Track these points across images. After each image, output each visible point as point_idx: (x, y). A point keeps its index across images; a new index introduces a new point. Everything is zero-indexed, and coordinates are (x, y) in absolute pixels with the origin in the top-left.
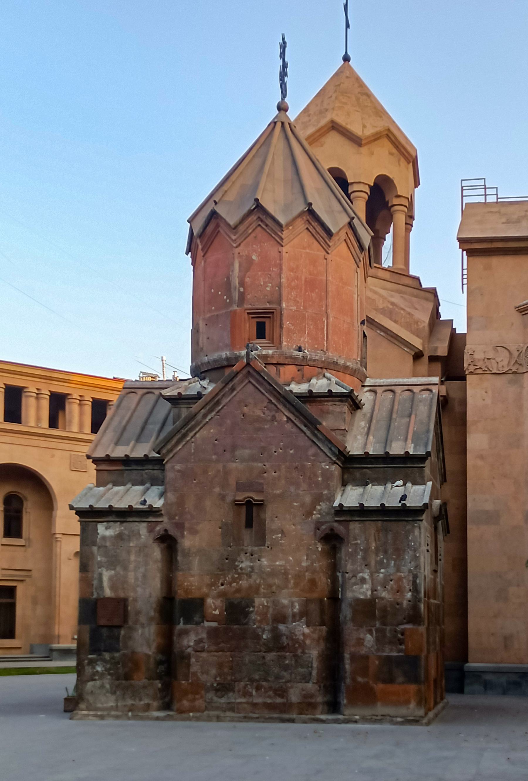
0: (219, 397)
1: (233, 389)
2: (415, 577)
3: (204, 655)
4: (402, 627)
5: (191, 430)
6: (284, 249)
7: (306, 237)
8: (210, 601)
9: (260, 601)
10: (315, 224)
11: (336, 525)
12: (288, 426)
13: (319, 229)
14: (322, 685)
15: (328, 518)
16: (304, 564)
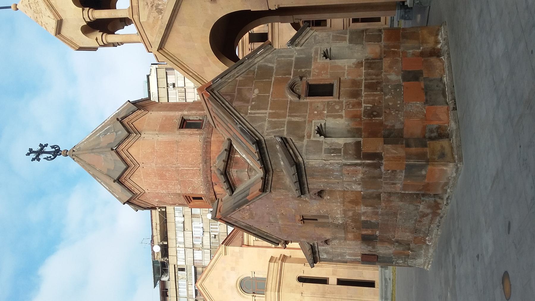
0: (242, 227)
1: (236, 222)
2: (345, 165)
3: (396, 236)
4: (383, 170)
5: (263, 234)
6: (146, 191)
7: (135, 179)
8: (364, 232)
9: (363, 218)
10: (125, 175)
11: (311, 193)
12: (252, 206)
13: (127, 172)
14: (422, 198)
15: (308, 195)
16: (339, 204)
